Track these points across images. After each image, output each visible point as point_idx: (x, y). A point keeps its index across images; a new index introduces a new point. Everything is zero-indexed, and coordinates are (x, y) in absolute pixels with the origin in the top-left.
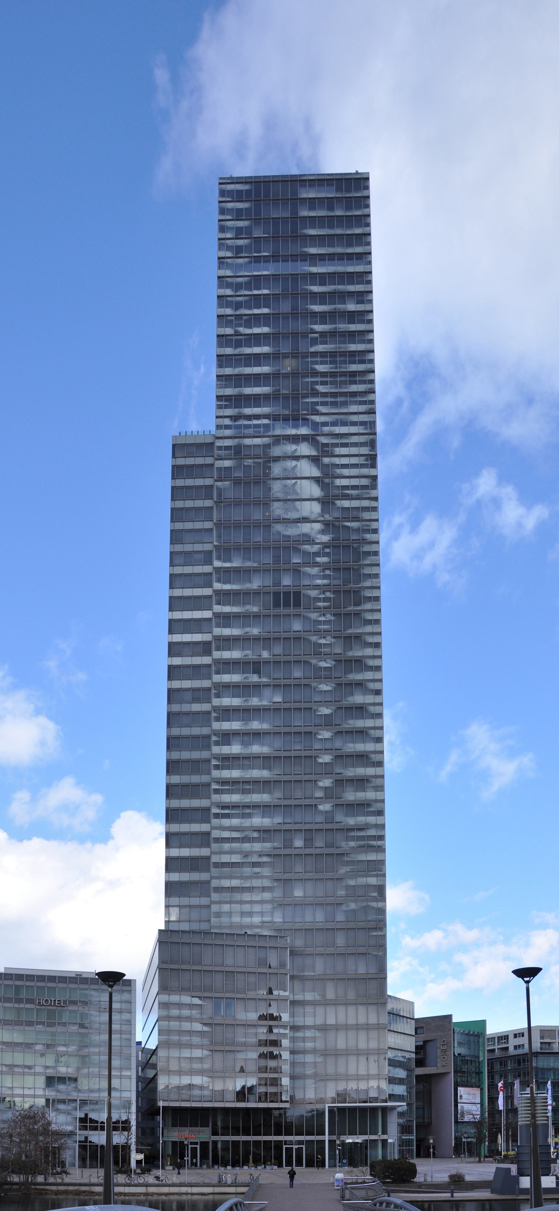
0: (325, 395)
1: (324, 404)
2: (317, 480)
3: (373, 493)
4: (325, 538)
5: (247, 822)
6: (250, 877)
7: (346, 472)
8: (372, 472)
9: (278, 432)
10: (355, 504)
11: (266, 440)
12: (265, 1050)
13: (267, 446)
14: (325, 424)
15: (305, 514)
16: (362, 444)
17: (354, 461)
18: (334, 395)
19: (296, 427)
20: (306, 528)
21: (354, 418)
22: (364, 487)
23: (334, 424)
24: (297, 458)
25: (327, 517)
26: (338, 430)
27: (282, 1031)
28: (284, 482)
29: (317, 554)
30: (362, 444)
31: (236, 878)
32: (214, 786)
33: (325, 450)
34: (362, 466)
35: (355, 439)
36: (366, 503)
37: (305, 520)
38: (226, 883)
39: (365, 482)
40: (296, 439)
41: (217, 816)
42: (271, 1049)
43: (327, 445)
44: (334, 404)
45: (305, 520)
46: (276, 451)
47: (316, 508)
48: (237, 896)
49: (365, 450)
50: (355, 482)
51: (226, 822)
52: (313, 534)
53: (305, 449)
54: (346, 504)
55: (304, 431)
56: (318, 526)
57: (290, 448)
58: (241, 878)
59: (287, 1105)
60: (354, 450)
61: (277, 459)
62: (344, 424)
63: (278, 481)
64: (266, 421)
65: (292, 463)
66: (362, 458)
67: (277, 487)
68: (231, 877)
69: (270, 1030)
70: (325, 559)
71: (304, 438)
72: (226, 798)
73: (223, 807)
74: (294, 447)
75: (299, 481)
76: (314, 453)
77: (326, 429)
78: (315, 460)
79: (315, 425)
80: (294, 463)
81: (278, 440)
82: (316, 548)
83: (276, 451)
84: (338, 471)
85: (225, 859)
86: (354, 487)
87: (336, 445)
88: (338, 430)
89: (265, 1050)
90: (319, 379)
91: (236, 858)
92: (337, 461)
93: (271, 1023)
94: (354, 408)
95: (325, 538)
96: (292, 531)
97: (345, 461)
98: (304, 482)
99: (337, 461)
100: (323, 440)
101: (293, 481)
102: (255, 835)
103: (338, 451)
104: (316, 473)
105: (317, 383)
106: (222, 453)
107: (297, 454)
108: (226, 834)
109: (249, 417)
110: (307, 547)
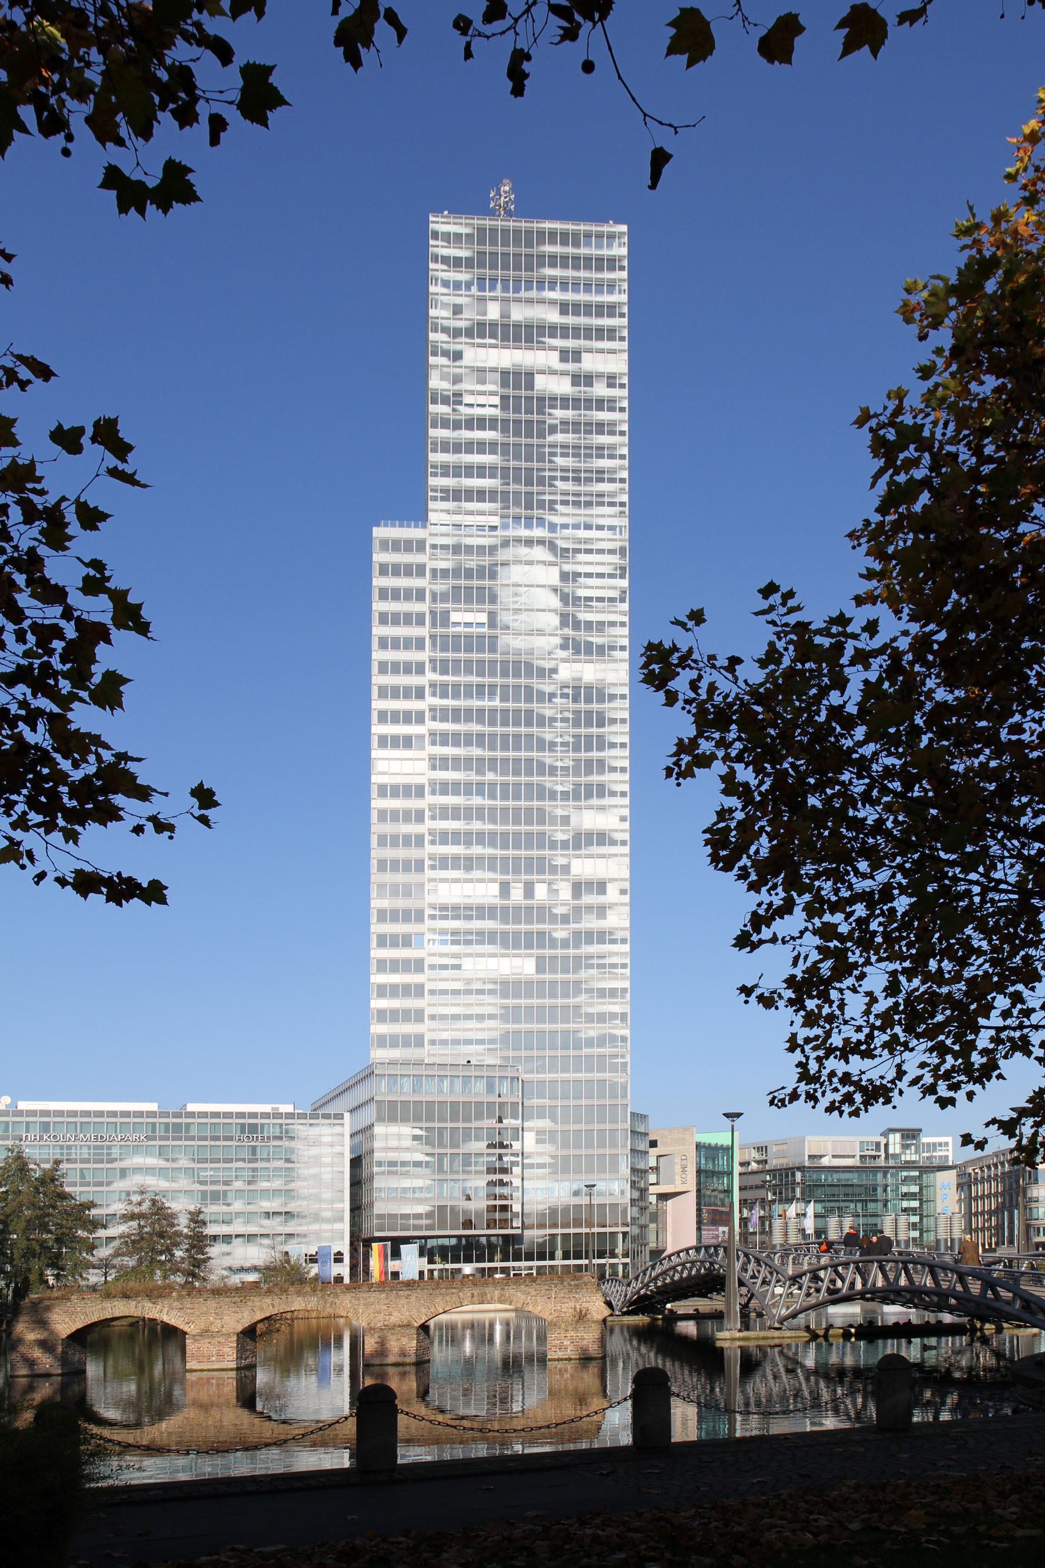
1: (565, 503)
7: (590, 582)
13: (493, 549)
14: (565, 526)
16: (611, 552)
22: (612, 600)
27: (513, 1159)
30: (611, 552)
34: (611, 576)
37: (541, 632)
40: (529, 542)
43: (567, 550)
45: (541, 632)
46: (502, 555)
53: (540, 553)
55: (538, 532)
57: (523, 551)
59: (519, 1231)
69: (500, 1157)
71: (541, 542)
77: (566, 532)
79: (553, 527)
81: (505, 544)
84: (582, 580)
100: (561, 544)
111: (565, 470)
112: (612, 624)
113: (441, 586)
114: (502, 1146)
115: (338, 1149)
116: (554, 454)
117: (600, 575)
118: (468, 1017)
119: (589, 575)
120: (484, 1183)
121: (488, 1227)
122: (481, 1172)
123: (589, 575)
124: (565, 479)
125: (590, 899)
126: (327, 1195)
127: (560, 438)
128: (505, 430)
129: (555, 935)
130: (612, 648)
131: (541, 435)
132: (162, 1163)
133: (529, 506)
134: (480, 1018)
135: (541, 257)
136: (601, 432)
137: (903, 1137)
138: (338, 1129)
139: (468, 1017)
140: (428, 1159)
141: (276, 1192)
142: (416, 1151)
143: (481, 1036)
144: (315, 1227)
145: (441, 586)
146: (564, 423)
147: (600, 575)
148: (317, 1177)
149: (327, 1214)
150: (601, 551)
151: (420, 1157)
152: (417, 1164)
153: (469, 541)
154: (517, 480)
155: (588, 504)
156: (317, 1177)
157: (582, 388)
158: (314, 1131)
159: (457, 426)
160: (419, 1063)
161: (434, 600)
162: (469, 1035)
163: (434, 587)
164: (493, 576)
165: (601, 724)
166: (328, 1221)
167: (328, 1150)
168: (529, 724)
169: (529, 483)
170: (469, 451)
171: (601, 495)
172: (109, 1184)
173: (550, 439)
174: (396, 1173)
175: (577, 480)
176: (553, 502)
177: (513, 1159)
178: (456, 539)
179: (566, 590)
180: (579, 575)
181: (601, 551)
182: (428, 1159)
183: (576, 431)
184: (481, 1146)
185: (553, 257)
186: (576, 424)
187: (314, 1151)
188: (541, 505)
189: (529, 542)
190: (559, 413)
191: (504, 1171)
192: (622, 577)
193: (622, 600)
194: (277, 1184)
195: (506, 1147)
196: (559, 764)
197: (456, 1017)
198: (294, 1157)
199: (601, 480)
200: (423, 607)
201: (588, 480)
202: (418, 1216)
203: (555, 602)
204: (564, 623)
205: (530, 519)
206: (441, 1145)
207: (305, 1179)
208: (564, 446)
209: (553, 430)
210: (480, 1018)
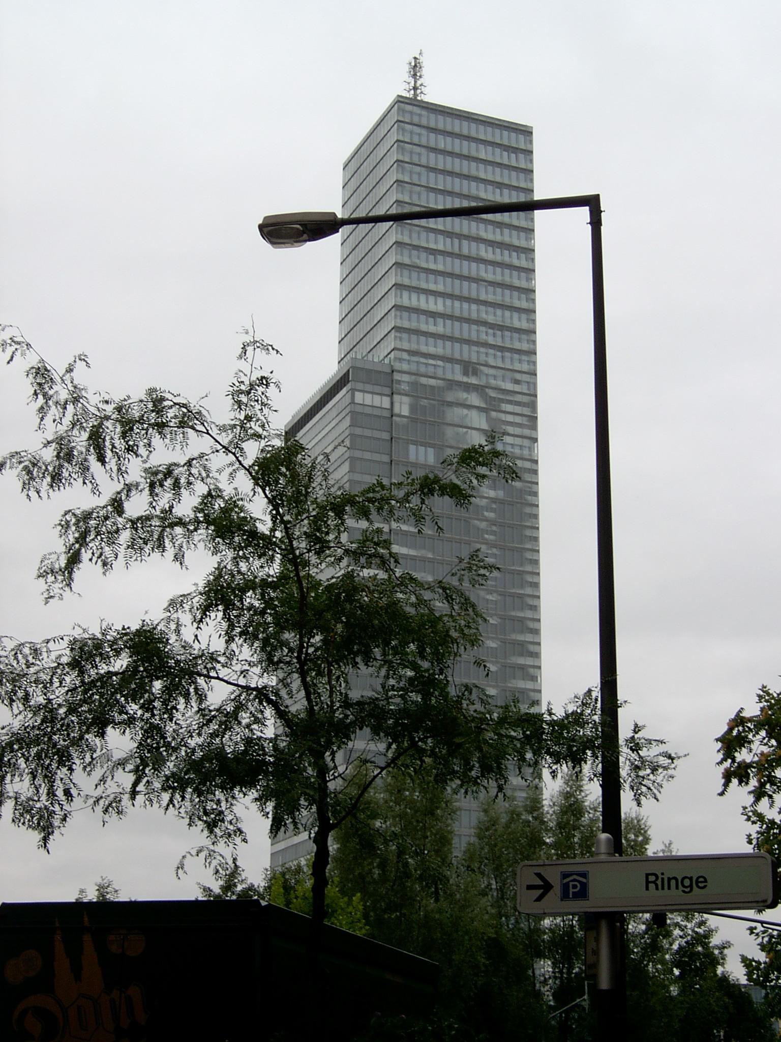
11: (441, 383)
17: (518, 420)
24: (469, 407)
28: (456, 429)
40: (467, 387)
49: (526, 411)
53: (474, 399)
57: (463, 396)
60: (518, 409)
61: (450, 404)
63: (451, 428)
66: (525, 419)
74: (465, 395)
75: (469, 431)
80: (465, 411)
83: (450, 397)
87: (502, 401)
92: (503, 417)
97: (510, 418)
98: (474, 432)
99: (503, 417)
100: (493, 394)
101: (465, 430)
103: (504, 407)
107: (468, 403)
117: (520, 425)
147: (520, 425)
178: (413, 377)
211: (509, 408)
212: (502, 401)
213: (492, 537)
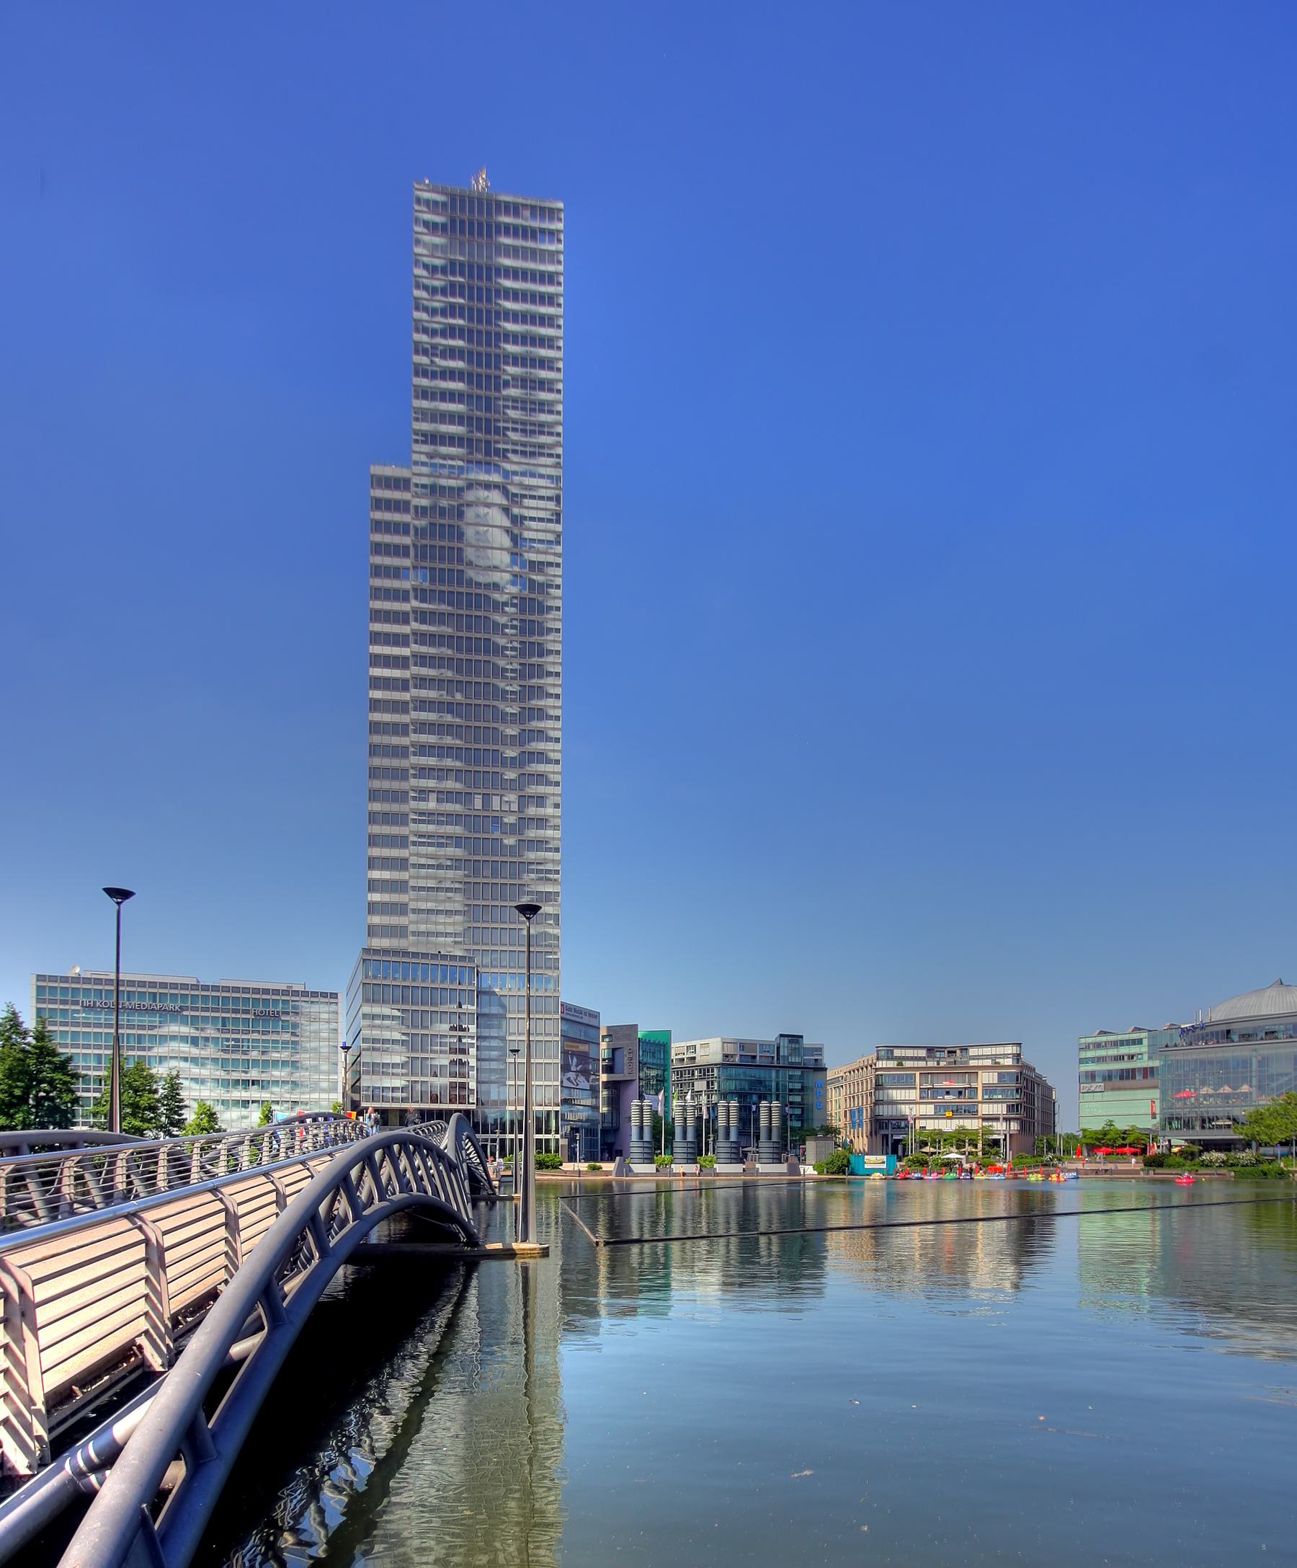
0: (515, 443)
1: (515, 452)
2: (507, 531)
3: (559, 549)
4: (514, 590)
5: (441, 851)
6: (444, 901)
7: (533, 525)
8: (559, 528)
9: (472, 476)
10: (541, 558)
12: (455, 1057)
13: (460, 490)
14: (515, 473)
15: (496, 563)
16: (550, 499)
17: (541, 514)
18: (524, 445)
19: (488, 472)
20: (496, 577)
21: (542, 471)
22: (549, 542)
23: (524, 474)
24: (489, 505)
25: (516, 569)
26: (528, 481)
27: (470, 1041)
29: (505, 604)
30: (550, 499)
31: (431, 901)
32: (413, 816)
33: (515, 499)
34: (549, 521)
35: (542, 493)
36: (551, 559)
38: (423, 906)
39: (551, 537)
40: (488, 486)
41: (414, 843)
42: (460, 1057)
43: (516, 495)
44: (524, 453)
45: (495, 568)
46: (470, 496)
47: (506, 558)
48: (433, 918)
49: (551, 505)
50: (541, 536)
51: (423, 850)
52: (502, 584)
53: (496, 497)
54: (533, 557)
55: (496, 478)
56: (507, 577)
57: (482, 494)
58: (436, 901)
60: (542, 504)
62: (533, 475)
64: (460, 463)
65: (483, 510)
67: (470, 532)
68: (427, 900)
69: (460, 1038)
70: (513, 610)
71: (497, 486)
72: (423, 828)
73: (420, 836)
74: (486, 493)
76: (505, 502)
77: (517, 479)
78: (506, 510)
79: (506, 474)
80: (486, 510)
81: (470, 486)
82: (505, 598)
85: (422, 883)
86: (541, 541)
87: (524, 496)
88: (528, 481)
89: (455, 1057)
90: (510, 425)
91: (431, 884)
93: (461, 1033)
94: (543, 460)
95: (514, 590)
96: (482, 578)
97: (533, 514)
99: (526, 513)
102: (449, 863)
103: (527, 502)
104: (507, 523)
105: (507, 429)
106: (419, 490)
107: (489, 501)
108: (423, 861)
109: (444, 457)
110: (497, 596)
111: (515, 422)
112: (550, 564)
113: (421, 523)
114: (462, 1029)
115: (333, 1026)
116: (506, 407)
117: (541, 520)
118: (438, 912)
119: (532, 519)
120: (446, 1062)
121: (451, 1102)
122: (445, 1052)
123: (532, 519)
124: (515, 430)
125: (532, 811)
126: (324, 1067)
127: (513, 392)
128: (470, 382)
129: (506, 842)
130: (550, 586)
131: (498, 389)
132: (194, 1033)
133: (488, 453)
134: (448, 913)
135: (498, 226)
136: (542, 389)
137: (790, 1042)
138: (333, 1007)
139: (438, 912)
140: (404, 1038)
141: (285, 1063)
142: (395, 1030)
143: (450, 929)
144: (315, 1096)
145: (421, 523)
146: (514, 378)
147: (541, 520)
148: (316, 1050)
149: (324, 1085)
150: (541, 498)
151: (397, 1036)
152: (394, 1042)
153: (443, 482)
154: (479, 429)
155: (533, 454)
156: (316, 1050)
157: (529, 349)
158: (315, 1008)
159: (434, 376)
160: (406, 954)
161: (416, 534)
162: (441, 929)
163: (417, 522)
164: (461, 515)
165: (541, 655)
166: (324, 1091)
167: (324, 1026)
168: (487, 652)
169: (488, 432)
170: (443, 399)
171: (542, 446)
172: (150, 1049)
173: (505, 392)
174: (378, 1050)
175: (524, 431)
176: (506, 451)
177: (470, 1041)
179: (516, 531)
180: (524, 518)
181: (541, 498)
182: (404, 1038)
183: (524, 387)
184: (445, 1028)
185: (507, 227)
186: (524, 380)
187: (314, 1027)
188: (497, 452)
189: (488, 486)
190: (511, 370)
191: (463, 1051)
192: (558, 521)
193: (558, 543)
194: (285, 1055)
195: (464, 1030)
196: (508, 688)
197: (429, 911)
198: (298, 1031)
199: (542, 433)
200: (407, 540)
201: (533, 432)
202: (394, 1089)
203: (507, 542)
204: (514, 562)
205: (488, 463)
206: (414, 1027)
207: (306, 1051)
208: (515, 400)
209: (506, 384)
210: (448, 913)
211: (533, 503)
212: (524, 496)
213: (513, 631)
